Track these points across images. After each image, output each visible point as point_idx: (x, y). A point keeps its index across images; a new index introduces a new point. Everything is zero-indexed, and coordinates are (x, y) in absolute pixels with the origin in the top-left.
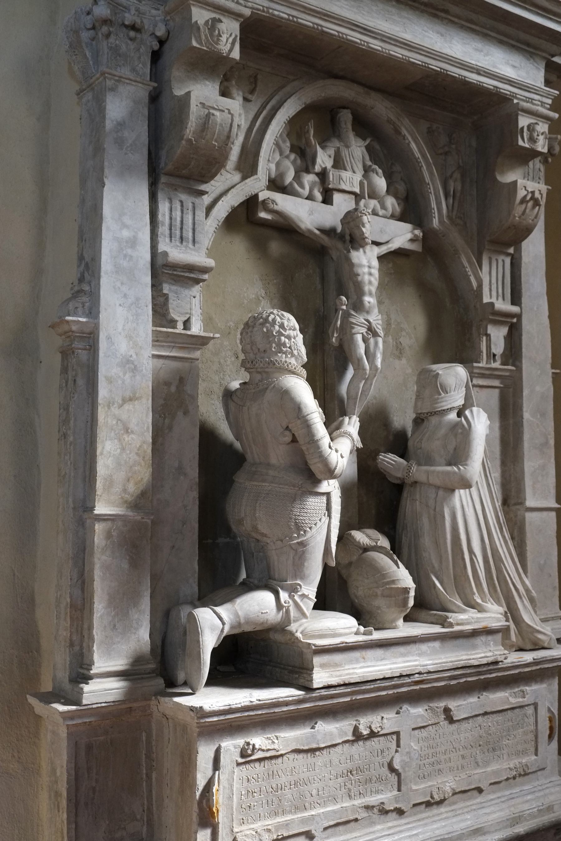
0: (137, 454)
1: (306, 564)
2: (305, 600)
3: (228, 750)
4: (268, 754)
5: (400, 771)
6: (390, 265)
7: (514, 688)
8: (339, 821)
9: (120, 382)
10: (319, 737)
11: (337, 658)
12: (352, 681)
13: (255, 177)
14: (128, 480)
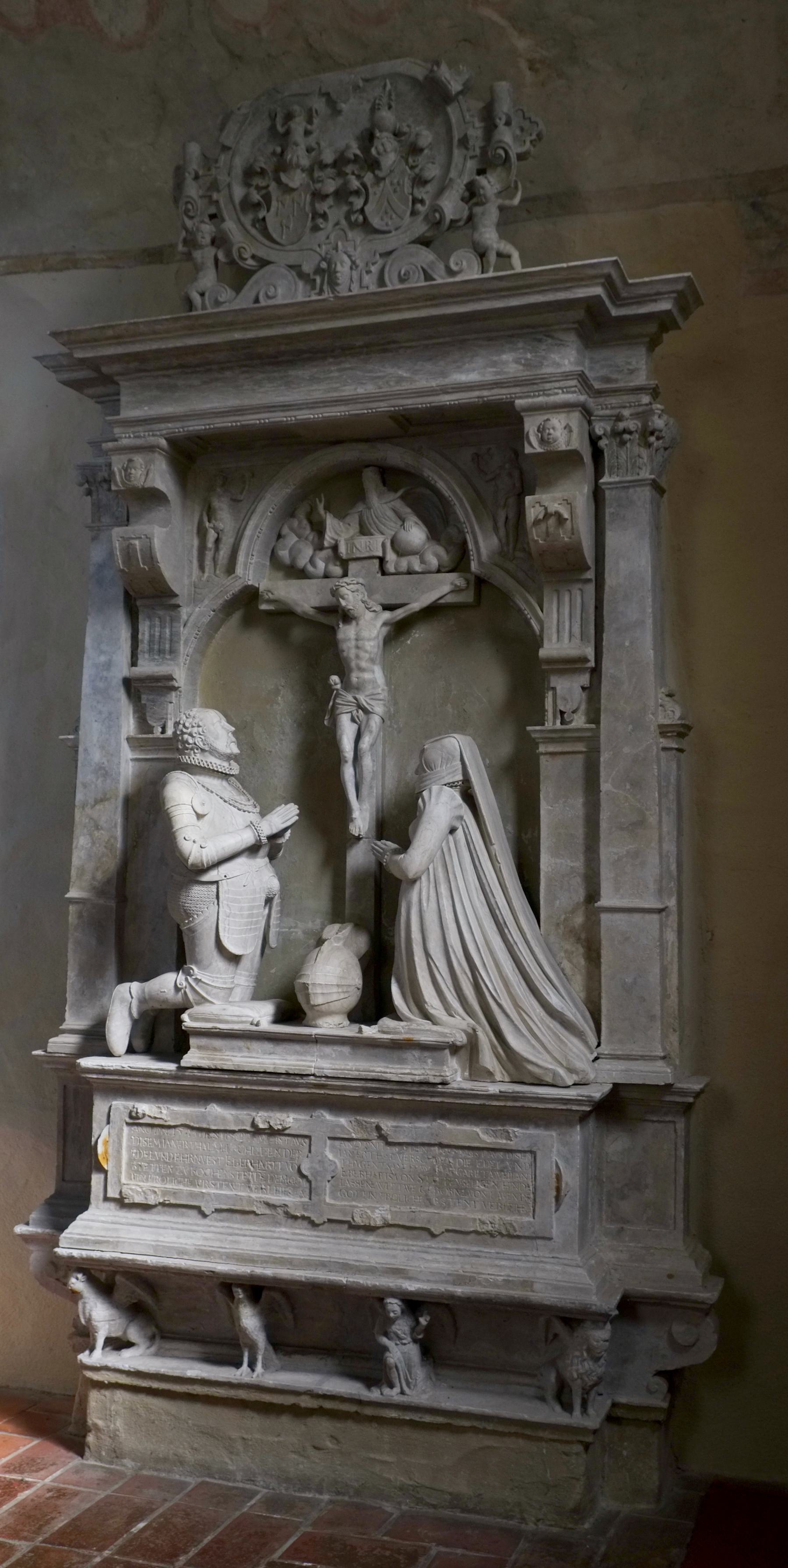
0: (105, 847)
1: (197, 949)
2: (200, 984)
3: (117, 1109)
4: (156, 1122)
5: (310, 1178)
6: (452, 622)
7: (495, 1126)
8: (232, 1207)
9: (93, 786)
10: (209, 1119)
11: (217, 1043)
12: (225, 1067)
13: (233, 576)
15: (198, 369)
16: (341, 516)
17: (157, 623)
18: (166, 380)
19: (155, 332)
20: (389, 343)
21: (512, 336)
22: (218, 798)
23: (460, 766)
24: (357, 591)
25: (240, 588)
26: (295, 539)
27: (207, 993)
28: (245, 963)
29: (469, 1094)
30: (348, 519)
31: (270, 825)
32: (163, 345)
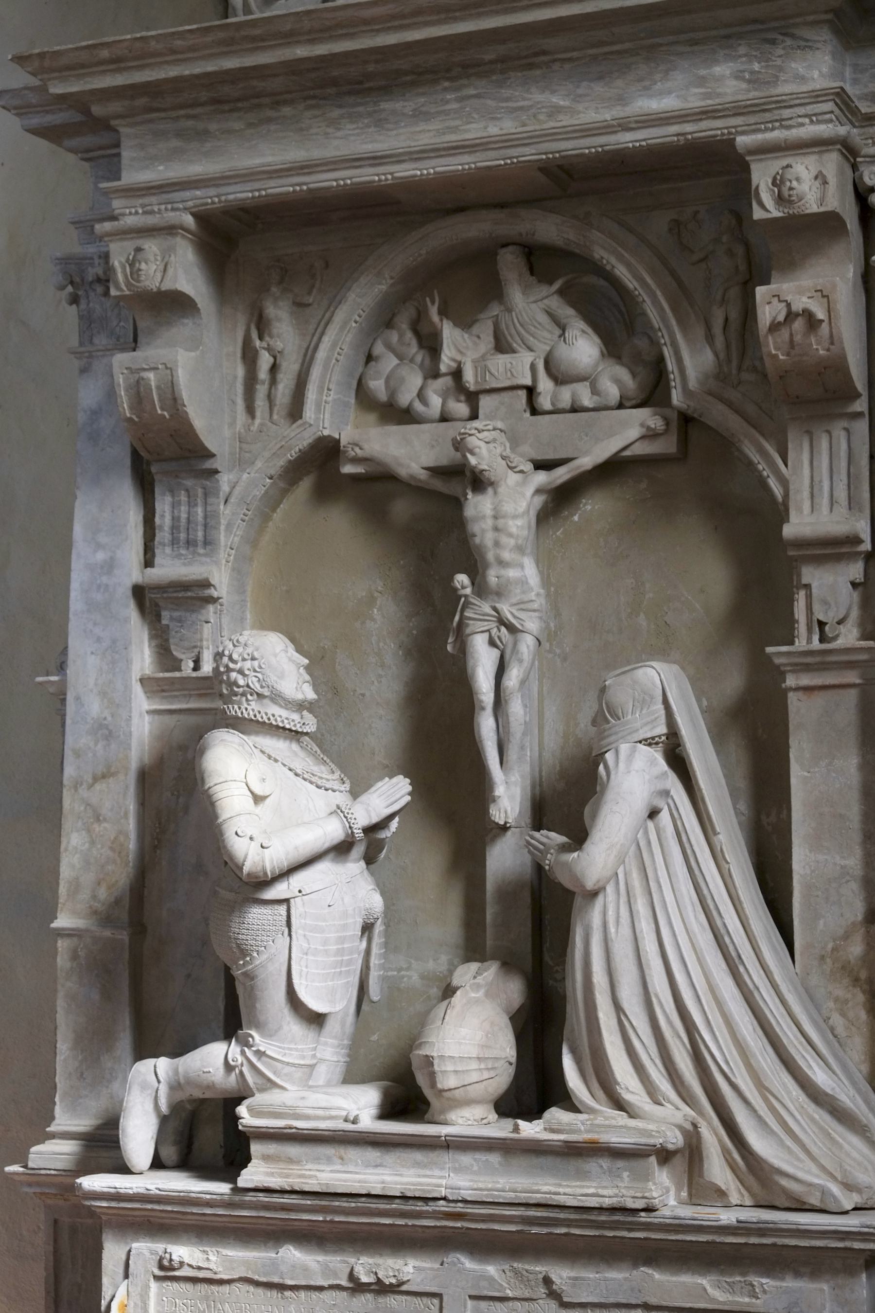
0: (111, 848)
1: (258, 1005)
2: (264, 1059)
3: (139, 1254)
4: (201, 1274)
6: (643, 485)
7: (731, 1275)
9: (90, 755)
10: (283, 1268)
11: (293, 1150)
13: (300, 422)
14: (99, 884)
15: (240, 105)
16: (465, 323)
17: (183, 497)
18: (190, 123)
19: (174, 52)
20: (536, 54)
21: (728, 37)
22: (286, 770)
23: (663, 712)
24: (494, 440)
25: (310, 441)
26: (395, 361)
27: (275, 1073)
28: (331, 1026)
29: (688, 1226)
30: (476, 329)
31: (368, 811)
32: (187, 70)
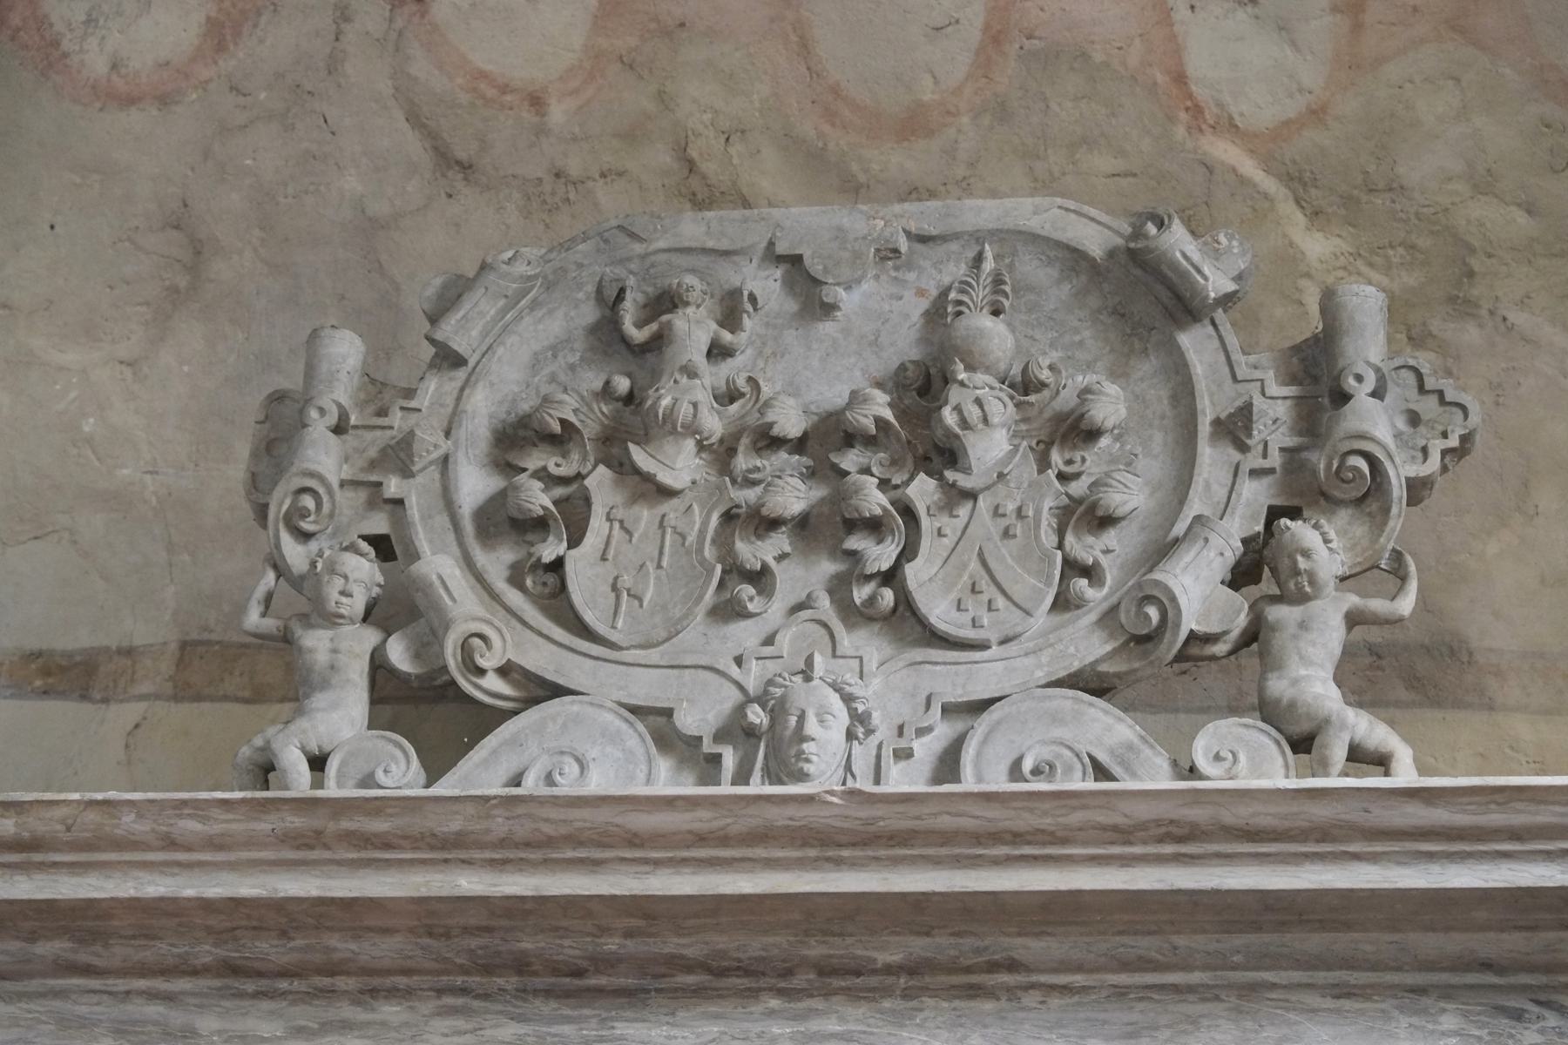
15: (283, 985)
18: (154, 1010)
19: (170, 843)
20: (993, 967)
21: (1420, 991)
32: (189, 887)
